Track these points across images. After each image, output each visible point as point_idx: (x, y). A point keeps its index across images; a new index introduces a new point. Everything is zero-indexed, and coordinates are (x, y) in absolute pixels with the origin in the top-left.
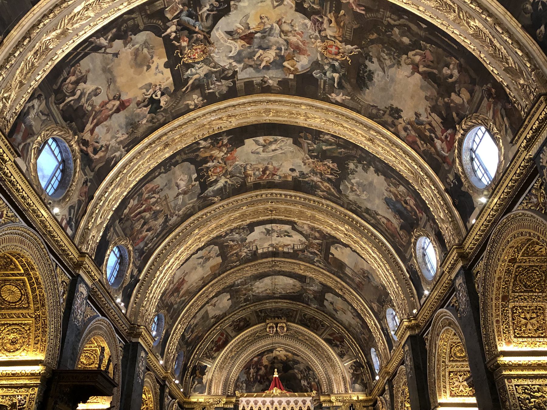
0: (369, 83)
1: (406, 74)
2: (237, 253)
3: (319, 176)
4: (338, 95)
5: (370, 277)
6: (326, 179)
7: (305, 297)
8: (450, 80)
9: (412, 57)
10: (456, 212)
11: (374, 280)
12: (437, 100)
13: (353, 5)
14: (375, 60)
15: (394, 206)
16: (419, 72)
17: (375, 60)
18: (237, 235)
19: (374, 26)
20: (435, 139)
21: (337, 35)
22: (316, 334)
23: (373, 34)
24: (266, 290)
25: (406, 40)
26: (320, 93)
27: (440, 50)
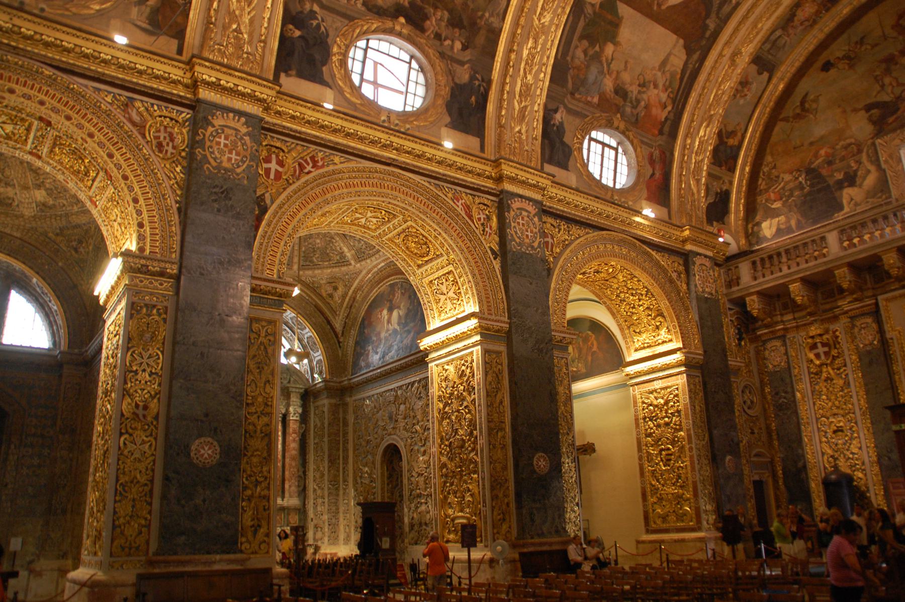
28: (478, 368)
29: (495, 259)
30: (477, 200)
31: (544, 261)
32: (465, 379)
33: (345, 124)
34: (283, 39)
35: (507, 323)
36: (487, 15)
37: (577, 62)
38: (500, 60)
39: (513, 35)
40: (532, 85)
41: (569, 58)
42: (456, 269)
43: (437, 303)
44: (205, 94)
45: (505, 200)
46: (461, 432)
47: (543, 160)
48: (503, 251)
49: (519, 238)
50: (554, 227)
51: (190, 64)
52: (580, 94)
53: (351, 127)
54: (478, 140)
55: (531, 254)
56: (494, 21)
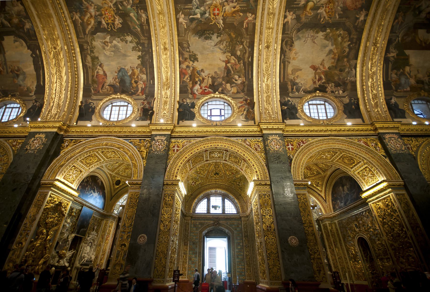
0: (203, 38)
1: (221, 58)
3: (97, 13)
4: (184, 19)
5: (21, 77)
6: (99, 20)
8: (234, 80)
9: (232, 59)
10: (177, 114)
11: (24, 80)
12: (218, 78)
13: (247, 20)
14: (219, 39)
15: (123, 76)
16: (226, 64)
17: (219, 39)
19: (239, 34)
20: (198, 85)
21: (226, 13)
23: (234, 34)
25: (239, 53)
26: (181, 6)
27: (243, 71)
28: (395, 202)
29: (386, 158)
30: (369, 139)
31: (410, 154)
32: (390, 207)
33: (309, 128)
34: (282, 111)
35: (402, 182)
36: (349, 78)
37: (394, 79)
38: (359, 90)
39: (362, 80)
40: (376, 94)
41: (389, 79)
42: (369, 165)
43: (364, 180)
44: (265, 132)
45: (381, 136)
46: (396, 230)
47: (393, 118)
48: (388, 154)
49: (394, 148)
50: (409, 140)
51: (258, 125)
52: (400, 90)
53: (312, 128)
54: (361, 119)
55: (403, 153)
56: (352, 79)
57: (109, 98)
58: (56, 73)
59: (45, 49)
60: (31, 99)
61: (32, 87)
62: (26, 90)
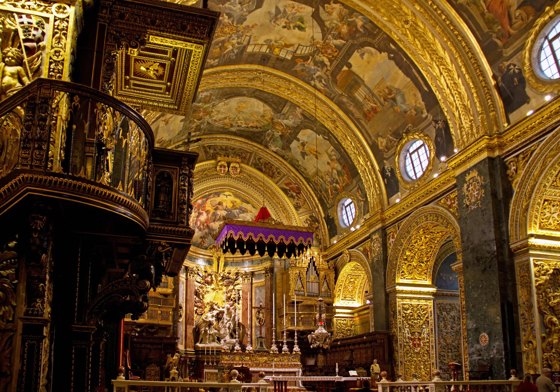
2: (223, 42)
5: (399, 98)
7: (268, 135)
18: (239, 6)
22: (272, 181)
24: (225, 118)
57: (534, 31)
58: (432, 59)
59: (398, 36)
60: (429, 122)
61: (420, 103)
62: (415, 112)
